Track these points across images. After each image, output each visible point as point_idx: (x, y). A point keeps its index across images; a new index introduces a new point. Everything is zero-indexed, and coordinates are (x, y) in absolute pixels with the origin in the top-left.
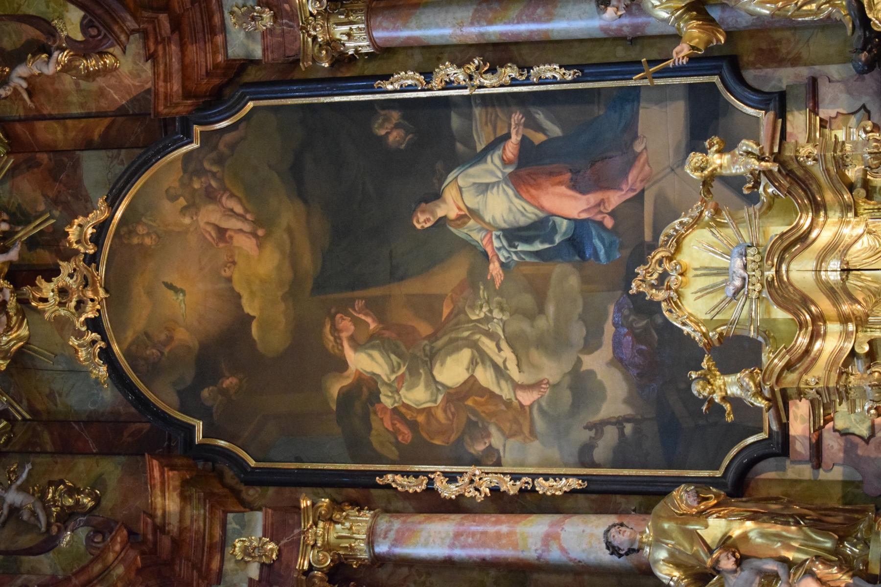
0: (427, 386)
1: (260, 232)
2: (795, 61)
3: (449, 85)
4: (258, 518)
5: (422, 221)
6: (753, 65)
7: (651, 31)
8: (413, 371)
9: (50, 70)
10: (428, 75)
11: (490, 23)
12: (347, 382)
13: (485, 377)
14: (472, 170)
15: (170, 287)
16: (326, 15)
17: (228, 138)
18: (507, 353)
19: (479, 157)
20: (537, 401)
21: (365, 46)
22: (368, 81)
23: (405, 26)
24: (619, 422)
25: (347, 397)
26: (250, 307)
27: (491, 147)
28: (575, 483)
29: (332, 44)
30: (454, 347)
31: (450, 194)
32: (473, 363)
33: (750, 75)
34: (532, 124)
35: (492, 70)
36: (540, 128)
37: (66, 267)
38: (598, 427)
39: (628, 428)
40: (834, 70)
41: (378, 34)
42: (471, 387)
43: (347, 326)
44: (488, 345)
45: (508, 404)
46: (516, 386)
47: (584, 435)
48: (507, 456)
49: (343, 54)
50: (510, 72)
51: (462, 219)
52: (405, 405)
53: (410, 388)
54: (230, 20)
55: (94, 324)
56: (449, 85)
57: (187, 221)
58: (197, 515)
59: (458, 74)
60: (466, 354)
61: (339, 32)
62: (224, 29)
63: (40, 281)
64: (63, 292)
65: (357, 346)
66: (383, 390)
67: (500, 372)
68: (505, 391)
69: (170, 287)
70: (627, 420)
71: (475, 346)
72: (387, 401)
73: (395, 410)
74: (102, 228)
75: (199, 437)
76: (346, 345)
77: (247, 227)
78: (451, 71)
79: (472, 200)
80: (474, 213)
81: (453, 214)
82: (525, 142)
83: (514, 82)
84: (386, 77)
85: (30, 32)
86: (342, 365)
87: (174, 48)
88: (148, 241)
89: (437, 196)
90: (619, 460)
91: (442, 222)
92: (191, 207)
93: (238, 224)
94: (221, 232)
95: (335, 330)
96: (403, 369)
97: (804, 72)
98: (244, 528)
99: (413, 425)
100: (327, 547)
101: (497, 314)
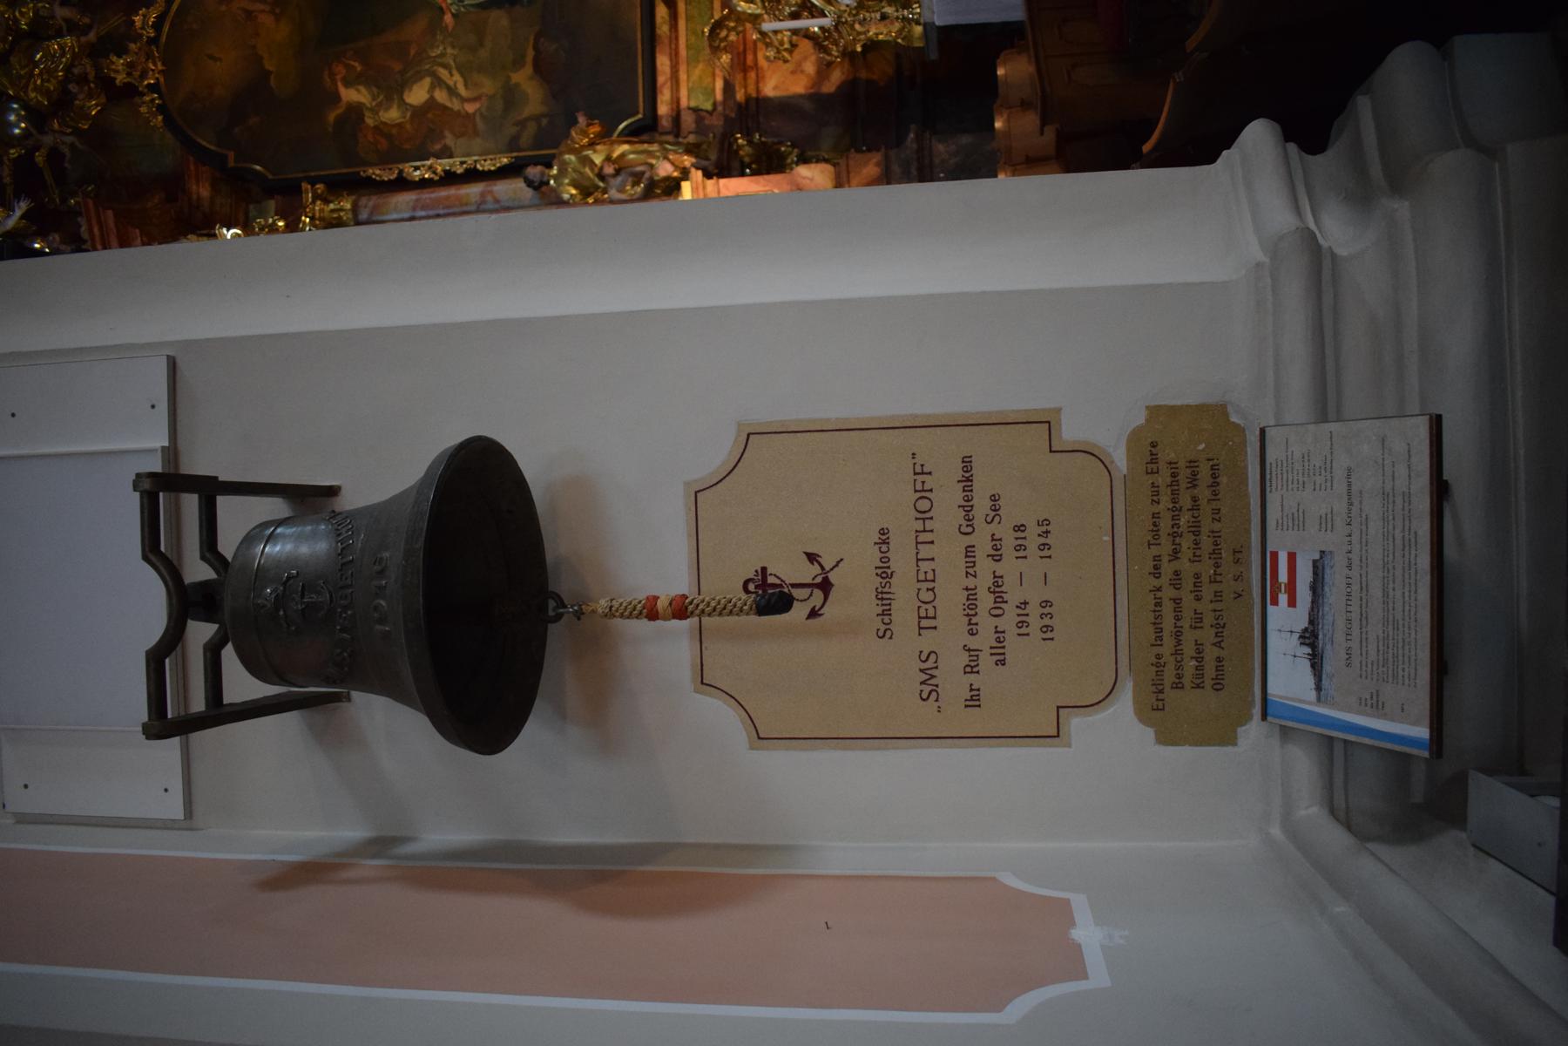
0: (399, 107)
1: (278, 11)
8: (389, 99)
12: (339, 111)
13: (441, 96)
15: (211, 57)
18: (457, 77)
20: (479, 109)
24: (537, 118)
26: (269, 65)
30: (418, 77)
32: (432, 88)
38: (522, 124)
42: (431, 104)
43: (340, 71)
44: (443, 73)
45: (458, 114)
46: (464, 100)
47: (513, 130)
52: (382, 122)
53: (387, 109)
57: (223, 8)
60: (427, 81)
65: (347, 85)
66: (367, 114)
67: (452, 91)
68: (455, 105)
69: (211, 57)
70: (543, 115)
71: (434, 75)
72: (370, 122)
73: (376, 128)
76: (339, 84)
77: (267, 8)
86: (337, 98)
95: (332, 75)
96: (381, 97)
101: (449, 51)
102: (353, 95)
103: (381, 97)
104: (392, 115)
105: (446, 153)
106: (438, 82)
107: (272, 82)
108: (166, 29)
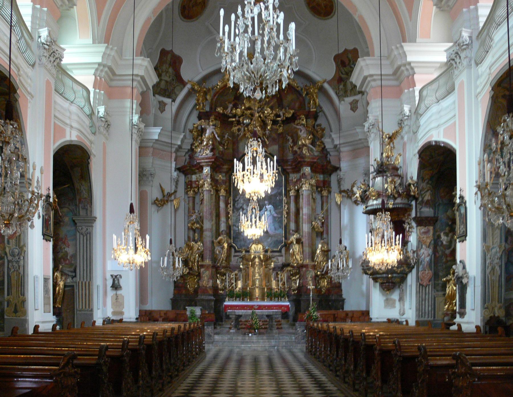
2: (285, 254)
4: (224, 178)
22: (286, 195)
28: (230, 224)
29: (291, 190)
39: (238, 231)
40: (284, 258)
78: (287, 206)
90: (234, 231)
97: (284, 255)
98: (223, 176)
100: (221, 189)
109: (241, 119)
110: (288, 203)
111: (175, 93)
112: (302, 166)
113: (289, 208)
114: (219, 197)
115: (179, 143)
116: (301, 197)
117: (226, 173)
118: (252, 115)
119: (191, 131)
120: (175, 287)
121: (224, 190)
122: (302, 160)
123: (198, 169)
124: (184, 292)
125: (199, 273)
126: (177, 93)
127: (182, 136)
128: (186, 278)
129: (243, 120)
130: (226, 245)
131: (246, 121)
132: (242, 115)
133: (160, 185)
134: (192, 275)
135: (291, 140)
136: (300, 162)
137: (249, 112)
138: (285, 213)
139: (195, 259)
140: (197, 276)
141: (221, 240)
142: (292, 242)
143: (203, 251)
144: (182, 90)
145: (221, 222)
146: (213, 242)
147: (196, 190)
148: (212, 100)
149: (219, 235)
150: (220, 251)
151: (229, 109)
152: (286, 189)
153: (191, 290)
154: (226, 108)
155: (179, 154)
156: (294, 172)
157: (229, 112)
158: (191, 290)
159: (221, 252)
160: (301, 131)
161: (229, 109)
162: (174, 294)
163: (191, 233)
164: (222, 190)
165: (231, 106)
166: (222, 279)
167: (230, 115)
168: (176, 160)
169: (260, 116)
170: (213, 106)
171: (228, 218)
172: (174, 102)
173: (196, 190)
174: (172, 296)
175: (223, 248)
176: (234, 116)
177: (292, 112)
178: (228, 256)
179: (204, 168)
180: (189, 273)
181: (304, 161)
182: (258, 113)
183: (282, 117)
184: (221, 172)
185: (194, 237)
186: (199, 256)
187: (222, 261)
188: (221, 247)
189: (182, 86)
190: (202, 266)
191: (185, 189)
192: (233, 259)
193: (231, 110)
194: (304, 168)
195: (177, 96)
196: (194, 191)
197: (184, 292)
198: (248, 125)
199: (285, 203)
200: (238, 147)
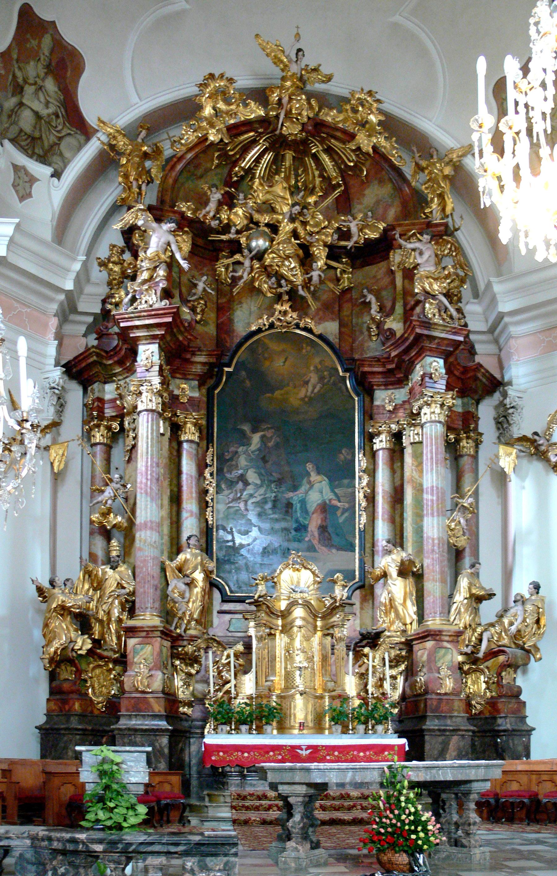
0: (247, 466)
1: (306, 399)
3: (360, 478)
4: (196, 394)
5: (309, 467)
6: (361, 593)
7: (376, 558)
8: (251, 460)
9: (373, 312)
10: (364, 471)
11: (383, 497)
12: (248, 432)
14: (328, 487)
16: (389, 432)
17: (344, 388)
18: (259, 498)
19: (333, 491)
20: (240, 510)
21: (375, 447)
22: (362, 448)
23: (383, 464)
24: (233, 540)
25: (243, 434)
27: (336, 495)
28: (210, 522)
29: (379, 434)
31: (319, 478)
33: (358, 592)
34: (345, 511)
35: (365, 497)
36: (343, 514)
37: (295, 315)
38: (231, 533)
41: (381, 453)
43: (269, 434)
48: (220, 496)
49: (373, 438)
50: (364, 504)
51: (309, 482)
52: (239, 456)
53: (246, 459)
54: (390, 392)
55: (272, 326)
56: (360, 478)
57: (312, 368)
58: (198, 369)
59: (365, 482)
60: (259, 482)
61: (383, 437)
62: (387, 389)
63: (289, 304)
64: (285, 313)
65: (262, 437)
66: (245, 448)
70: (234, 543)
71: (261, 486)
72: (240, 449)
74: (310, 331)
75: (226, 369)
76: (262, 433)
77: (309, 394)
79: (317, 486)
80: (311, 487)
81: (312, 479)
82: (337, 508)
83: (360, 505)
84: (364, 455)
85: (389, 305)
86: (255, 430)
87: (380, 369)
88: (304, 351)
89: (319, 473)
91: (308, 474)
92: (317, 370)
93: (310, 390)
94: (307, 383)
95: (268, 428)
96: (253, 456)
98: (192, 388)
99: (231, 459)
102: (256, 439)
103: (253, 456)
104: (243, 461)
105: (219, 490)
106: (258, 487)
107: (268, 395)
108: (303, 333)
109: (243, 240)
110: (372, 472)
111: (61, 155)
112: (420, 354)
113: (372, 485)
114: (180, 444)
115: (69, 286)
116: (408, 452)
117: (202, 380)
118: (274, 228)
119: (103, 264)
120: (53, 692)
121: (195, 425)
122: (426, 332)
123: (121, 363)
124: (77, 706)
125: (124, 655)
126: (67, 154)
127: (77, 266)
128: (83, 666)
129: (249, 238)
130: (199, 576)
131: (260, 243)
132: (247, 228)
133: (10, 392)
134: (101, 657)
135: (375, 307)
136: (419, 337)
137: (265, 219)
138: (360, 496)
139: (109, 613)
140: (116, 662)
141: (186, 561)
142: (385, 575)
143: (133, 593)
144: (80, 148)
145: (184, 515)
146: (163, 570)
147: (115, 425)
148: (164, 179)
149: (179, 551)
150: (184, 592)
151: (212, 207)
152: (363, 432)
153: (99, 700)
154: (203, 201)
155: (68, 328)
156: (387, 385)
157: (212, 214)
158: (99, 700)
159: (187, 595)
160: (421, 253)
161: (212, 207)
162: (49, 715)
163: (99, 543)
164: (189, 425)
165: (216, 196)
166: (189, 675)
167: (214, 224)
168: (60, 337)
169: (295, 234)
170: (167, 198)
171: (204, 505)
172: (59, 179)
173: (115, 425)
174: (42, 720)
175: (191, 584)
176: (226, 228)
177: (382, 226)
178: (206, 610)
179: (141, 348)
180: (90, 652)
181: (431, 338)
182: (292, 220)
183: (355, 239)
184: (185, 377)
185: (108, 552)
186: (122, 605)
187: (189, 622)
188: (187, 580)
189: (82, 138)
190: (131, 631)
191: (84, 423)
192: (216, 619)
193: (218, 211)
194: (429, 360)
195: (66, 163)
196: (109, 428)
197: (77, 706)
198: (260, 256)
199: (361, 471)
200: (230, 321)
